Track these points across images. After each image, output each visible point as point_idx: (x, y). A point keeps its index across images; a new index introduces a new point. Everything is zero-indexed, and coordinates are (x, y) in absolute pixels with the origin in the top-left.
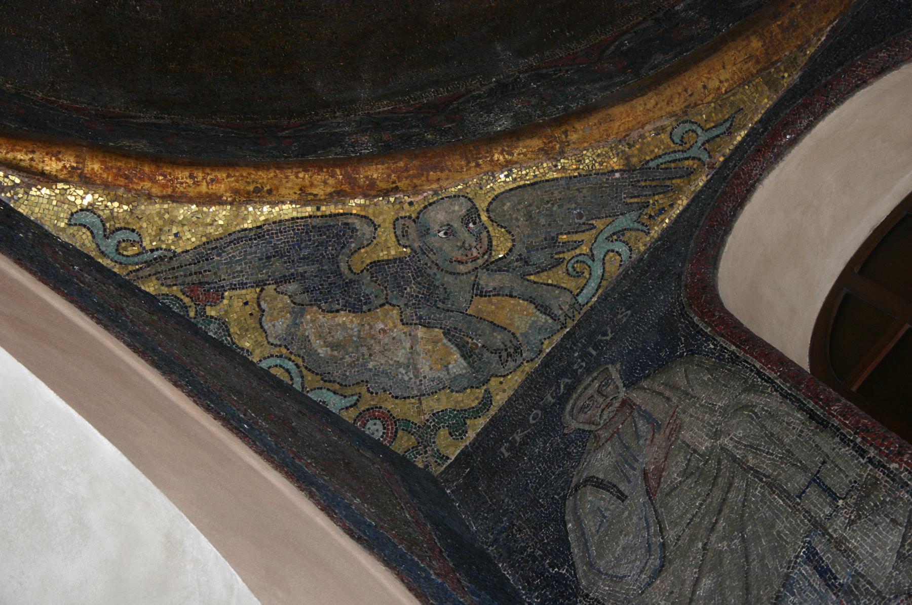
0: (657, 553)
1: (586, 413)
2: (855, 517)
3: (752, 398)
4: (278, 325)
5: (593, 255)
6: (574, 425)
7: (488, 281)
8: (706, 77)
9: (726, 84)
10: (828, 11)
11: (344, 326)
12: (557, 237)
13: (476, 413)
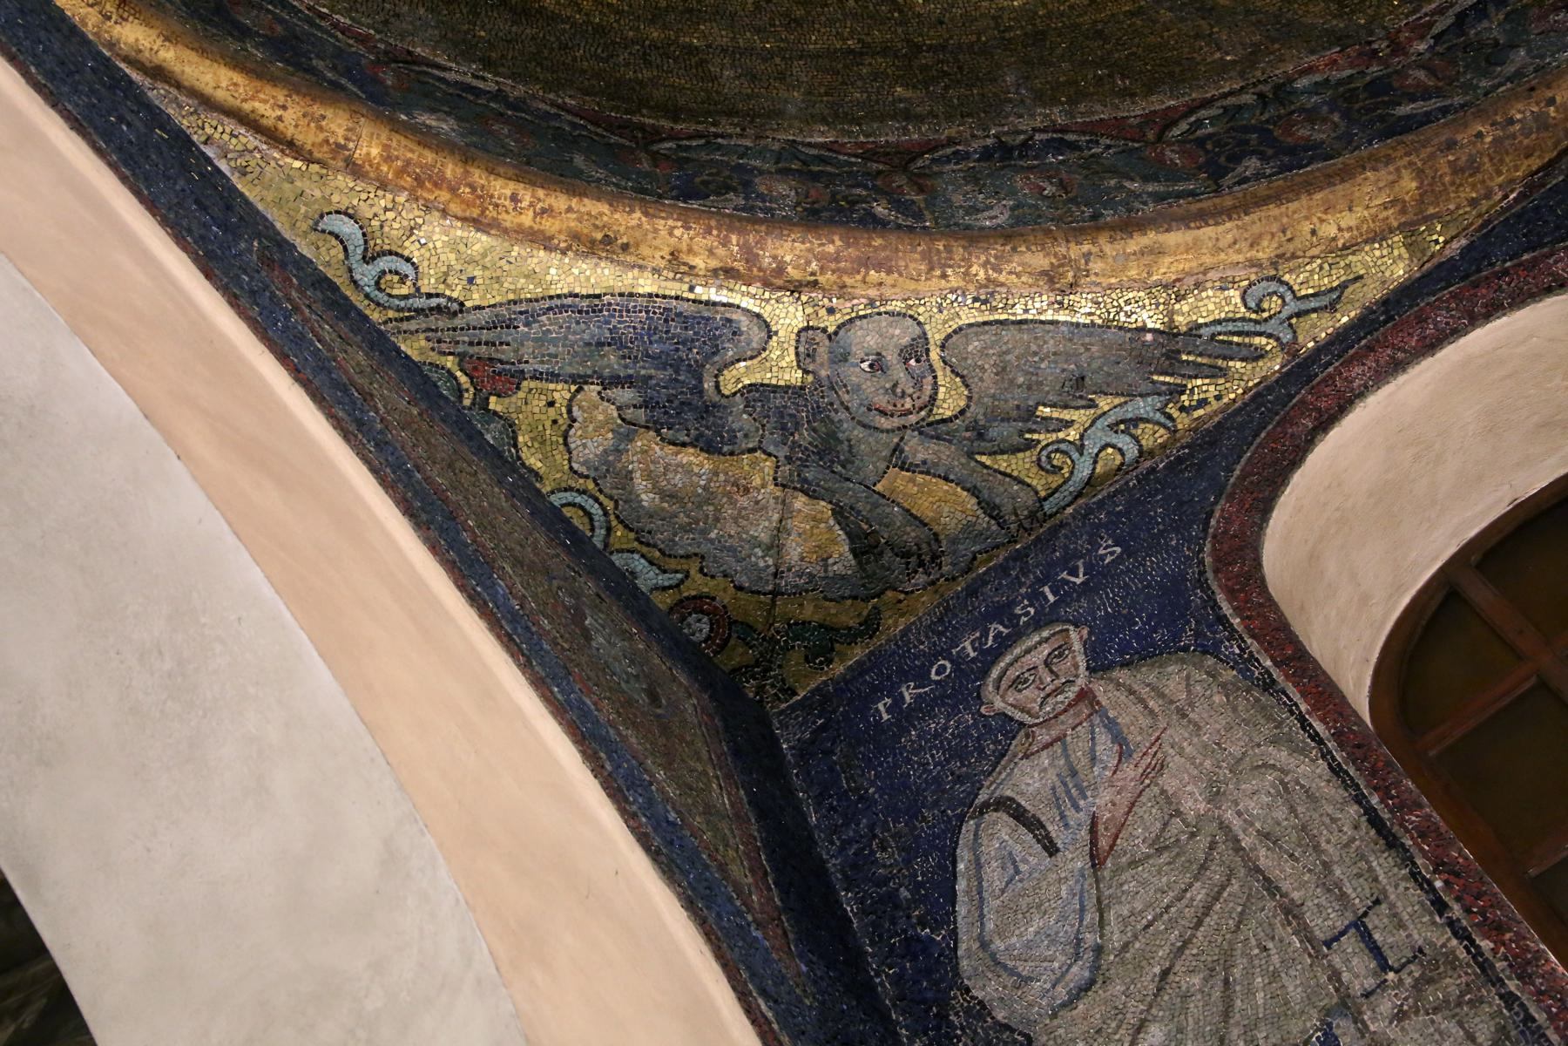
0: (1089, 955)
1: (1020, 691)
2: (1410, 1008)
3: (1281, 756)
4: (590, 445)
5: (1083, 446)
6: (999, 704)
7: (918, 449)
8: (1319, 218)
9: (1347, 235)
10: (1531, 155)
11: (687, 470)
12: (1036, 408)
13: (852, 637)
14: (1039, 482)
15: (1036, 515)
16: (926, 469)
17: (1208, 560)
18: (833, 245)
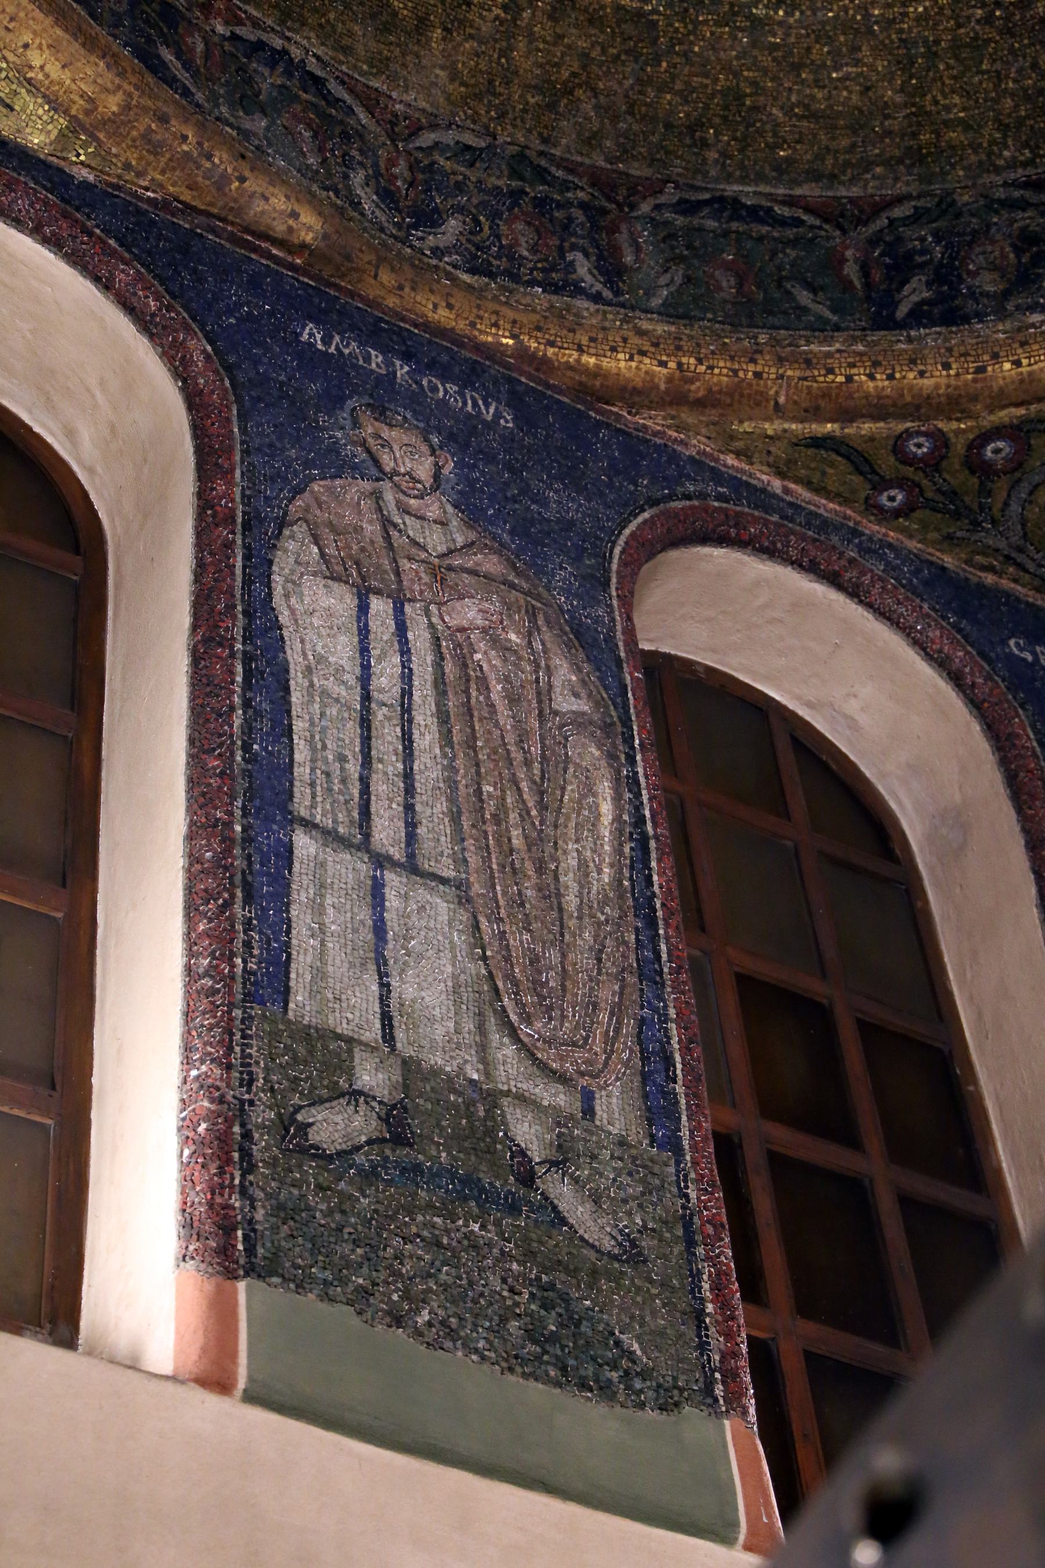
9: (40, 76)
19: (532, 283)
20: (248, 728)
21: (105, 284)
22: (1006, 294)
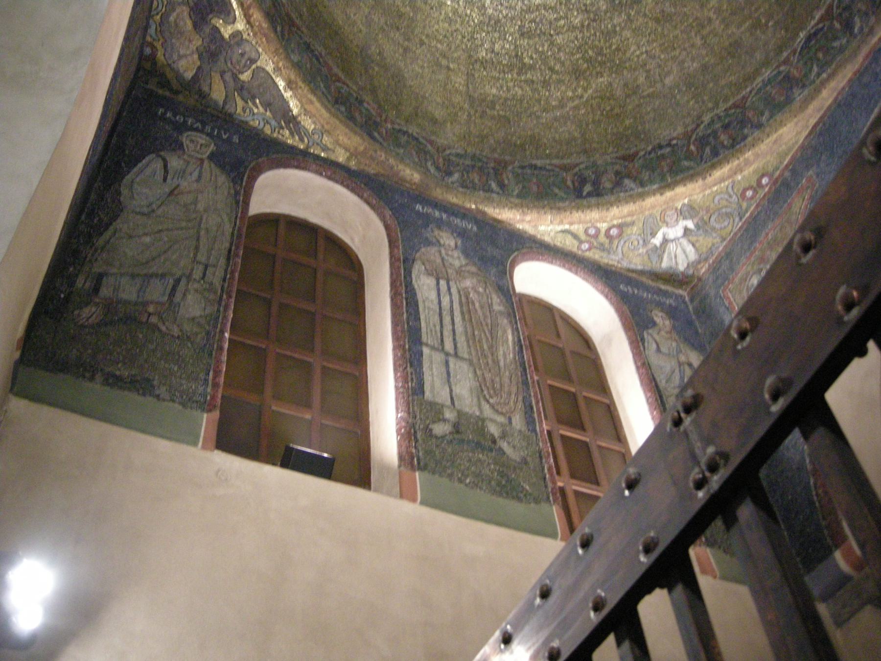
0: (150, 209)
3: (226, 220)
6: (184, 140)
7: (228, 76)
11: (185, 24)
13: (171, 90)
14: (239, 110)
15: (231, 115)
16: (224, 82)
17: (252, 165)
18: (265, 25)
19: (479, 190)
20: (408, 318)
21: (361, 197)
22: (613, 188)
